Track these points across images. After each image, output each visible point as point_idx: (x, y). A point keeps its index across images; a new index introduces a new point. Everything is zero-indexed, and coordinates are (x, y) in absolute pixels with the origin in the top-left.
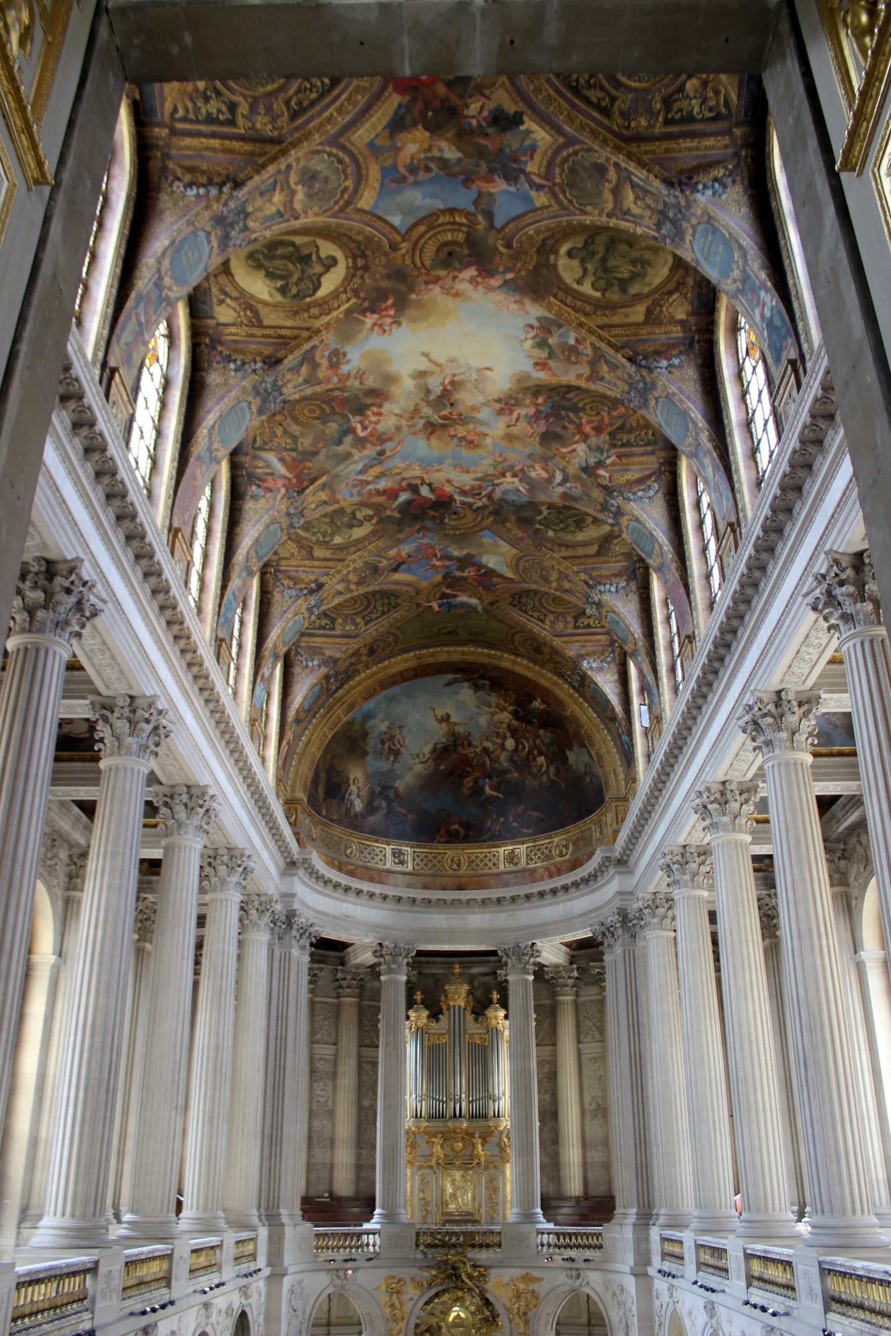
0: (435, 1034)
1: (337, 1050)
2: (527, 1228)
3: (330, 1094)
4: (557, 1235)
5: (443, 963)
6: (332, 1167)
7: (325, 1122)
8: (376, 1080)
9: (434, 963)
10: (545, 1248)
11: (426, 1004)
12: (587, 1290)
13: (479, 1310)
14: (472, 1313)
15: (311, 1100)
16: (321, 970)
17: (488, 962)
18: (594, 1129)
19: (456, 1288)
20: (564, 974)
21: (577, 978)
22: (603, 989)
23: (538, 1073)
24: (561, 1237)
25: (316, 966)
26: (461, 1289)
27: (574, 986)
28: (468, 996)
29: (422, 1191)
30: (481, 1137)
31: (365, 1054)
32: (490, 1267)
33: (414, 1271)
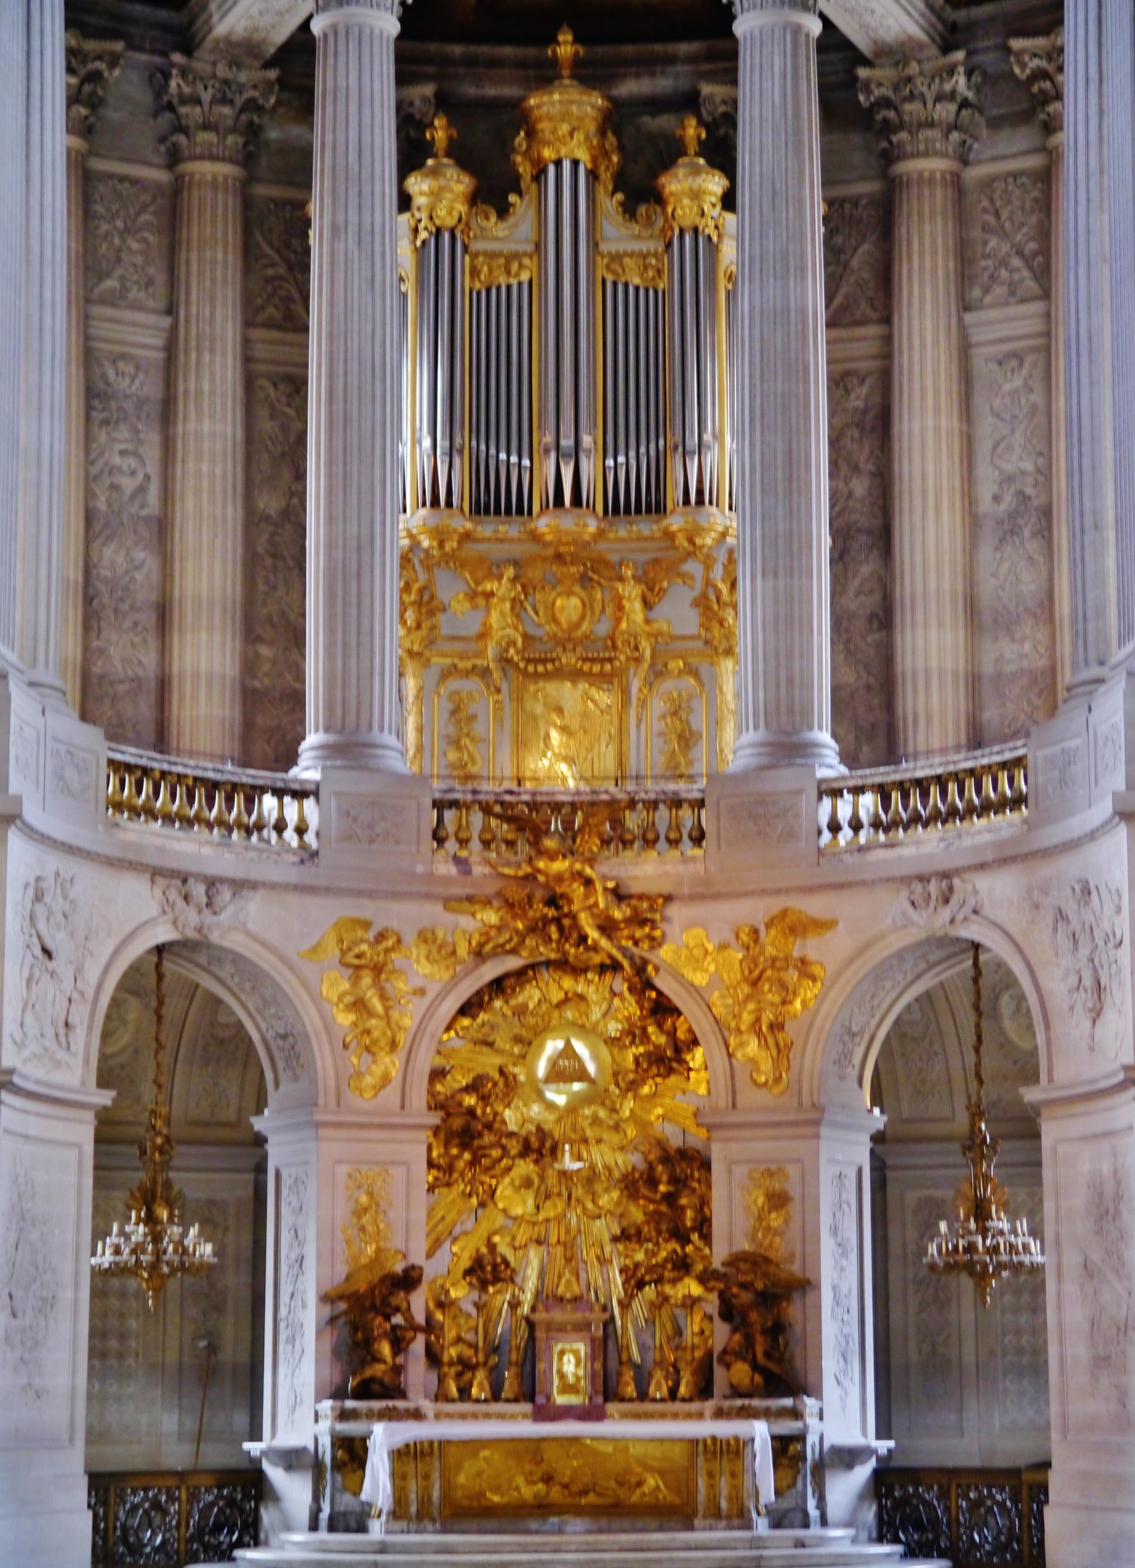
0: (491, 256)
1: (173, 331)
2: (785, 779)
3: (153, 468)
4: (883, 792)
5: (521, 64)
6: (163, 686)
7: (140, 555)
8: (304, 433)
9: (494, 63)
10: (846, 834)
11: (462, 155)
12: (972, 931)
13: (635, 1033)
14: (611, 1042)
15: (89, 482)
16: (114, 61)
17: (671, 60)
18: (1009, 574)
19: (562, 965)
20: (921, 85)
21: (965, 104)
22: (1051, 127)
23: (832, 414)
24: (896, 796)
25: (91, 45)
26: (578, 971)
27: (955, 126)
28: (602, 133)
29: (457, 744)
30: (637, 579)
31: (261, 351)
32: (668, 898)
33: (432, 913)
